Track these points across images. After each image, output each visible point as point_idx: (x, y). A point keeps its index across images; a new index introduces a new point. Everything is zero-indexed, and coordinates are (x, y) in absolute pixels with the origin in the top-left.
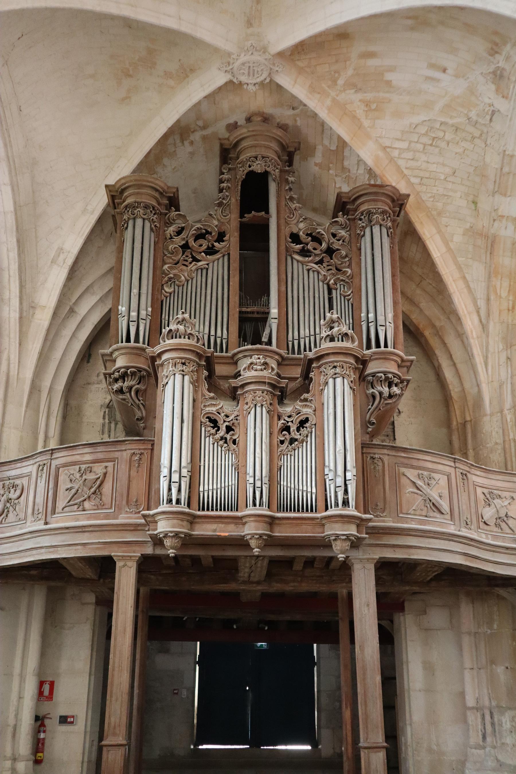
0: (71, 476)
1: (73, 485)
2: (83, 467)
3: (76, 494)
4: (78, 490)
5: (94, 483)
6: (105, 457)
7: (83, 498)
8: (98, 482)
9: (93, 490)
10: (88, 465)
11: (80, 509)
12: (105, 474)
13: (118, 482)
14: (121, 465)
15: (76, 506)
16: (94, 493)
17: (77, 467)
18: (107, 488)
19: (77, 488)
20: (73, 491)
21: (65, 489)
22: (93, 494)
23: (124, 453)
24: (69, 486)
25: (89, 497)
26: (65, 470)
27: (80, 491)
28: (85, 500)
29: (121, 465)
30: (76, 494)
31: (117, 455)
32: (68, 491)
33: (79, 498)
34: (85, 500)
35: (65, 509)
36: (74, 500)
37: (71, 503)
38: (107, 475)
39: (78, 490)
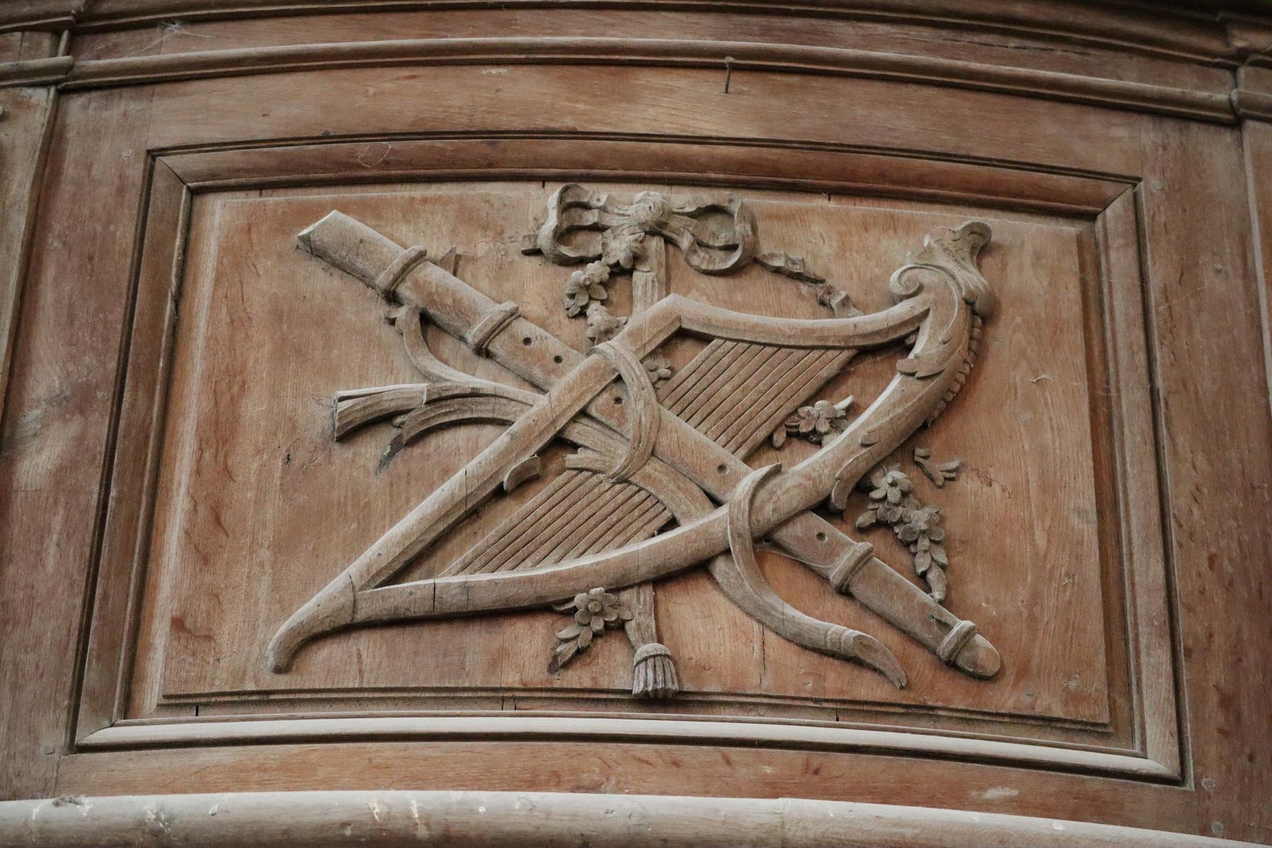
0: (434, 275)
1: (459, 378)
2: (633, 205)
3: (525, 481)
4: (561, 443)
5: (826, 389)
6: (948, 141)
7: (643, 549)
8: (887, 400)
9: (812, 468)
10: (685, 199)
11: (621, 669)
12: (982, 313)
13: (1182, 440)
14: (1187, 270)
15: (529, 646)
16: (844, 503)
17: (542, 206)
18: (1027, 467)
19: (535, 411)
20: (475, 457)
21: (319, 417)
22: (823, 508)
23: (1216, 149)
24: (402, 386)
25: (765, 541)
26: (316, 211)
27: (600, 449)
28: (698, 569)
29: (1187, 270)
30: (525, 481)
31: (1113, 143)
32: (374, 447)
33: (569, 542)
34: (698, 569)
35: (329, 654)
36: (513, 549)
37: (415, 589)
38: (1007, 339)
39: (561, 443)
